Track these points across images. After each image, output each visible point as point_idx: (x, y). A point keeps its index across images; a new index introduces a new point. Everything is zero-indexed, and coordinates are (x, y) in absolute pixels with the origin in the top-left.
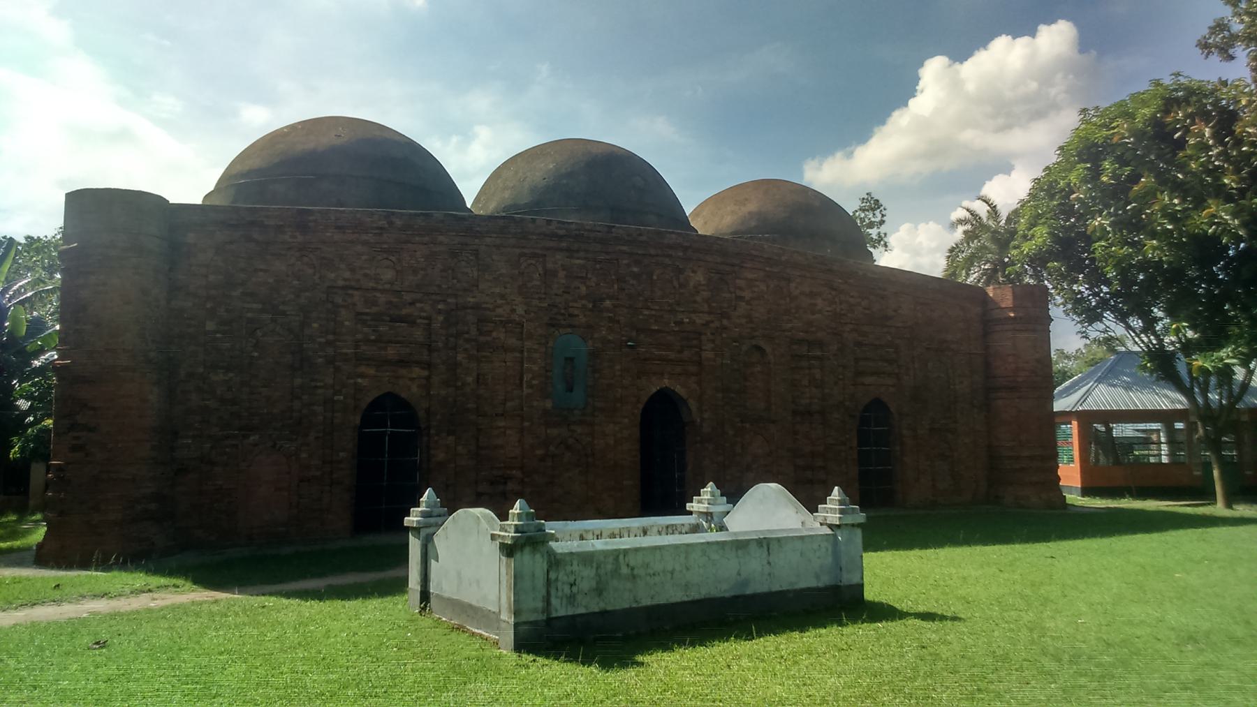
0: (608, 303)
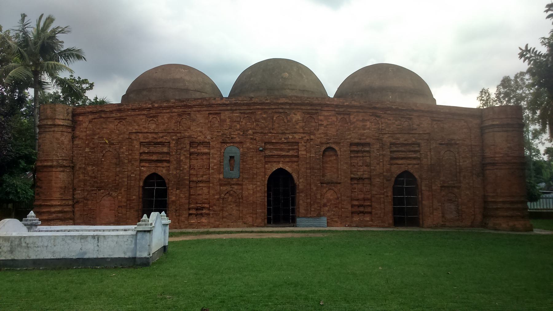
0: (250, 132)
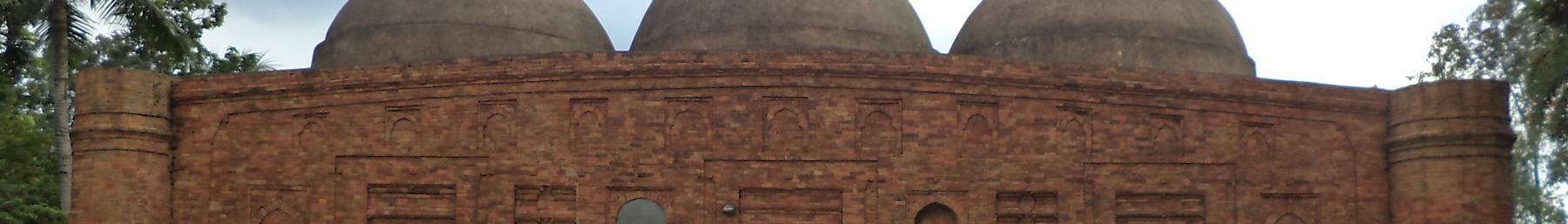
0: (697, 157)
